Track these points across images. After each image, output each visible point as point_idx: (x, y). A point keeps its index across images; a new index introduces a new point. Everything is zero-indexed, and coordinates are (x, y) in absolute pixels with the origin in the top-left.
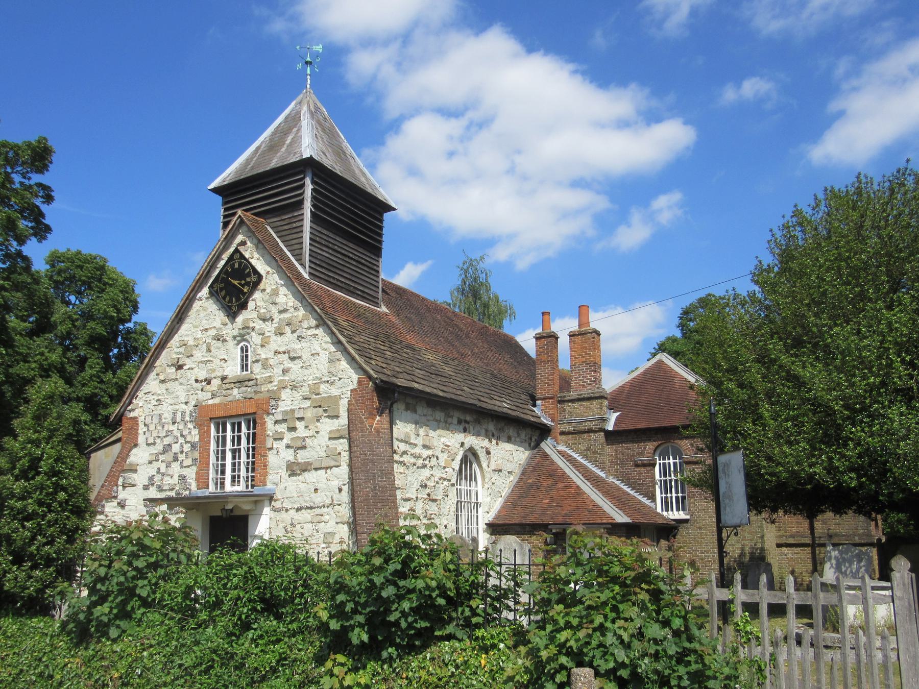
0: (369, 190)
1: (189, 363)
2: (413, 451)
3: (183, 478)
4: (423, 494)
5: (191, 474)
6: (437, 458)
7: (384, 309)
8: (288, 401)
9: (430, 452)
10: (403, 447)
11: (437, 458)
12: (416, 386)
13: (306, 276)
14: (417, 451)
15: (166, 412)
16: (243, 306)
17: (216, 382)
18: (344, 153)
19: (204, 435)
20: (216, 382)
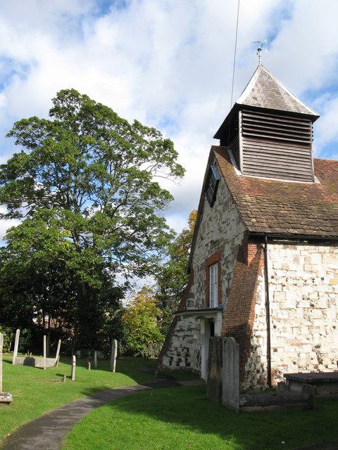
0: (294, 110)
1: (205, 236)
2: (293, 276)
3: (203, 300)
4: (307, 304)
5: (203, 297)
6: (323, 279)
7: (317, 181)
8: (227, 252)
9: (314, 275)
10: (280, 274)
11: (323, 279)
12: (292, 231)
13: (238, 173)
14: (298, 275)
15: (199, 263)
16: (214, 199)
17: (210, 244)
18: (278, 93)
19: (208, 276)
20: (210, 244)
